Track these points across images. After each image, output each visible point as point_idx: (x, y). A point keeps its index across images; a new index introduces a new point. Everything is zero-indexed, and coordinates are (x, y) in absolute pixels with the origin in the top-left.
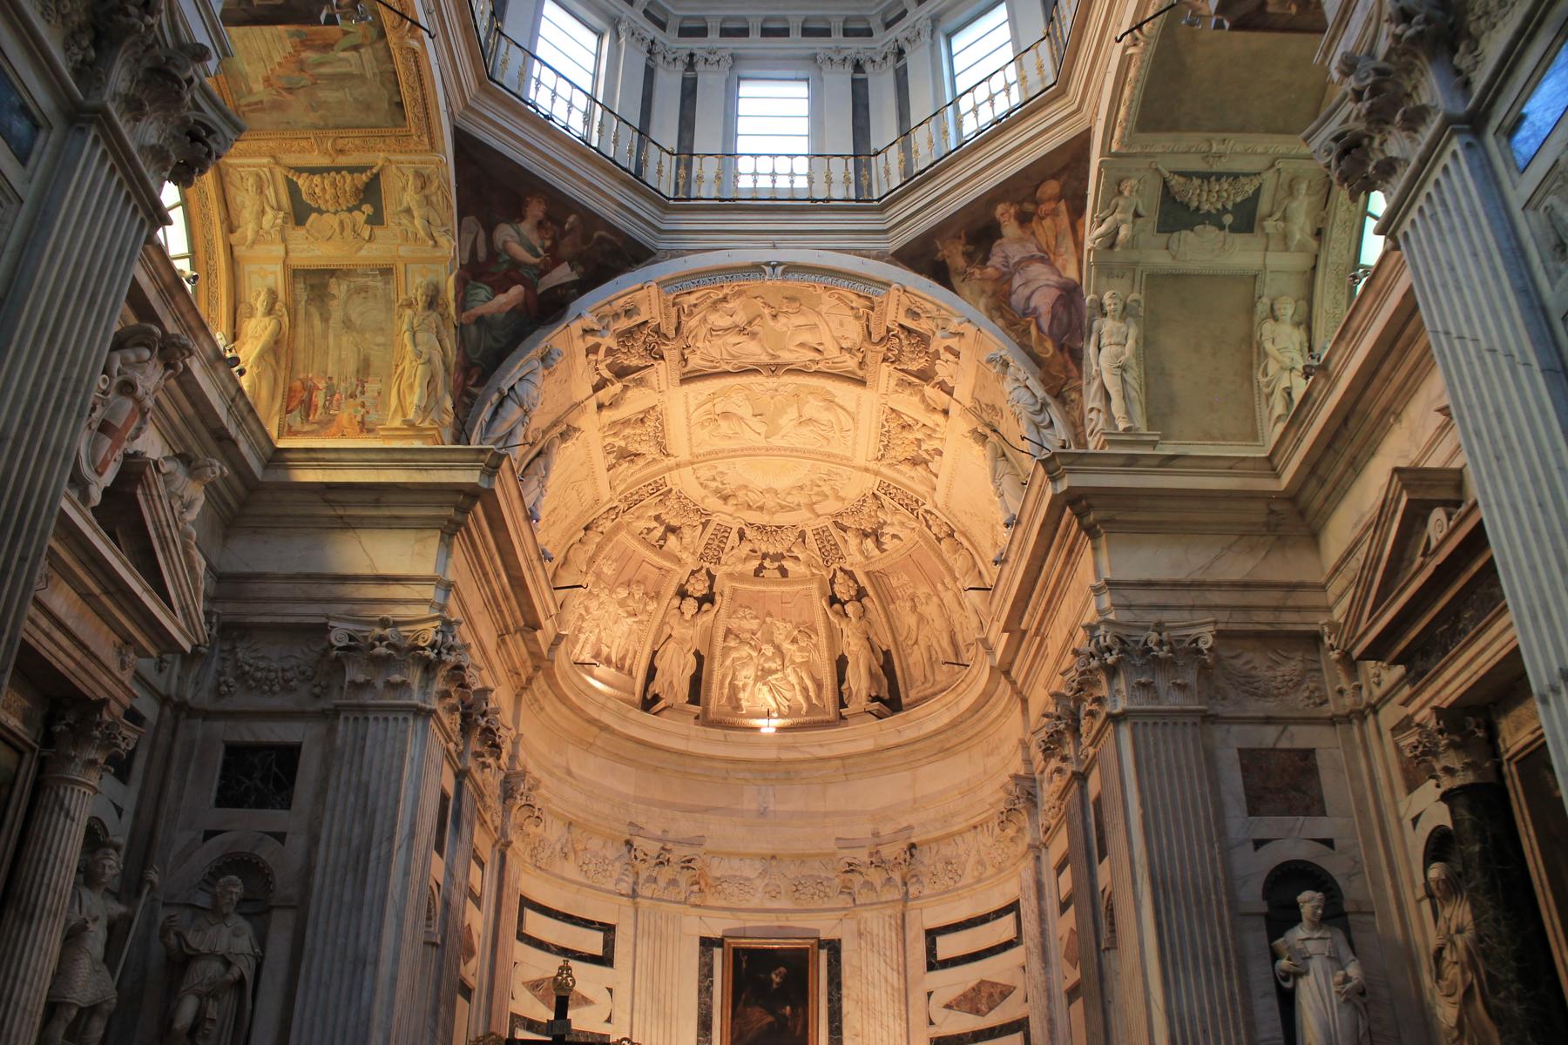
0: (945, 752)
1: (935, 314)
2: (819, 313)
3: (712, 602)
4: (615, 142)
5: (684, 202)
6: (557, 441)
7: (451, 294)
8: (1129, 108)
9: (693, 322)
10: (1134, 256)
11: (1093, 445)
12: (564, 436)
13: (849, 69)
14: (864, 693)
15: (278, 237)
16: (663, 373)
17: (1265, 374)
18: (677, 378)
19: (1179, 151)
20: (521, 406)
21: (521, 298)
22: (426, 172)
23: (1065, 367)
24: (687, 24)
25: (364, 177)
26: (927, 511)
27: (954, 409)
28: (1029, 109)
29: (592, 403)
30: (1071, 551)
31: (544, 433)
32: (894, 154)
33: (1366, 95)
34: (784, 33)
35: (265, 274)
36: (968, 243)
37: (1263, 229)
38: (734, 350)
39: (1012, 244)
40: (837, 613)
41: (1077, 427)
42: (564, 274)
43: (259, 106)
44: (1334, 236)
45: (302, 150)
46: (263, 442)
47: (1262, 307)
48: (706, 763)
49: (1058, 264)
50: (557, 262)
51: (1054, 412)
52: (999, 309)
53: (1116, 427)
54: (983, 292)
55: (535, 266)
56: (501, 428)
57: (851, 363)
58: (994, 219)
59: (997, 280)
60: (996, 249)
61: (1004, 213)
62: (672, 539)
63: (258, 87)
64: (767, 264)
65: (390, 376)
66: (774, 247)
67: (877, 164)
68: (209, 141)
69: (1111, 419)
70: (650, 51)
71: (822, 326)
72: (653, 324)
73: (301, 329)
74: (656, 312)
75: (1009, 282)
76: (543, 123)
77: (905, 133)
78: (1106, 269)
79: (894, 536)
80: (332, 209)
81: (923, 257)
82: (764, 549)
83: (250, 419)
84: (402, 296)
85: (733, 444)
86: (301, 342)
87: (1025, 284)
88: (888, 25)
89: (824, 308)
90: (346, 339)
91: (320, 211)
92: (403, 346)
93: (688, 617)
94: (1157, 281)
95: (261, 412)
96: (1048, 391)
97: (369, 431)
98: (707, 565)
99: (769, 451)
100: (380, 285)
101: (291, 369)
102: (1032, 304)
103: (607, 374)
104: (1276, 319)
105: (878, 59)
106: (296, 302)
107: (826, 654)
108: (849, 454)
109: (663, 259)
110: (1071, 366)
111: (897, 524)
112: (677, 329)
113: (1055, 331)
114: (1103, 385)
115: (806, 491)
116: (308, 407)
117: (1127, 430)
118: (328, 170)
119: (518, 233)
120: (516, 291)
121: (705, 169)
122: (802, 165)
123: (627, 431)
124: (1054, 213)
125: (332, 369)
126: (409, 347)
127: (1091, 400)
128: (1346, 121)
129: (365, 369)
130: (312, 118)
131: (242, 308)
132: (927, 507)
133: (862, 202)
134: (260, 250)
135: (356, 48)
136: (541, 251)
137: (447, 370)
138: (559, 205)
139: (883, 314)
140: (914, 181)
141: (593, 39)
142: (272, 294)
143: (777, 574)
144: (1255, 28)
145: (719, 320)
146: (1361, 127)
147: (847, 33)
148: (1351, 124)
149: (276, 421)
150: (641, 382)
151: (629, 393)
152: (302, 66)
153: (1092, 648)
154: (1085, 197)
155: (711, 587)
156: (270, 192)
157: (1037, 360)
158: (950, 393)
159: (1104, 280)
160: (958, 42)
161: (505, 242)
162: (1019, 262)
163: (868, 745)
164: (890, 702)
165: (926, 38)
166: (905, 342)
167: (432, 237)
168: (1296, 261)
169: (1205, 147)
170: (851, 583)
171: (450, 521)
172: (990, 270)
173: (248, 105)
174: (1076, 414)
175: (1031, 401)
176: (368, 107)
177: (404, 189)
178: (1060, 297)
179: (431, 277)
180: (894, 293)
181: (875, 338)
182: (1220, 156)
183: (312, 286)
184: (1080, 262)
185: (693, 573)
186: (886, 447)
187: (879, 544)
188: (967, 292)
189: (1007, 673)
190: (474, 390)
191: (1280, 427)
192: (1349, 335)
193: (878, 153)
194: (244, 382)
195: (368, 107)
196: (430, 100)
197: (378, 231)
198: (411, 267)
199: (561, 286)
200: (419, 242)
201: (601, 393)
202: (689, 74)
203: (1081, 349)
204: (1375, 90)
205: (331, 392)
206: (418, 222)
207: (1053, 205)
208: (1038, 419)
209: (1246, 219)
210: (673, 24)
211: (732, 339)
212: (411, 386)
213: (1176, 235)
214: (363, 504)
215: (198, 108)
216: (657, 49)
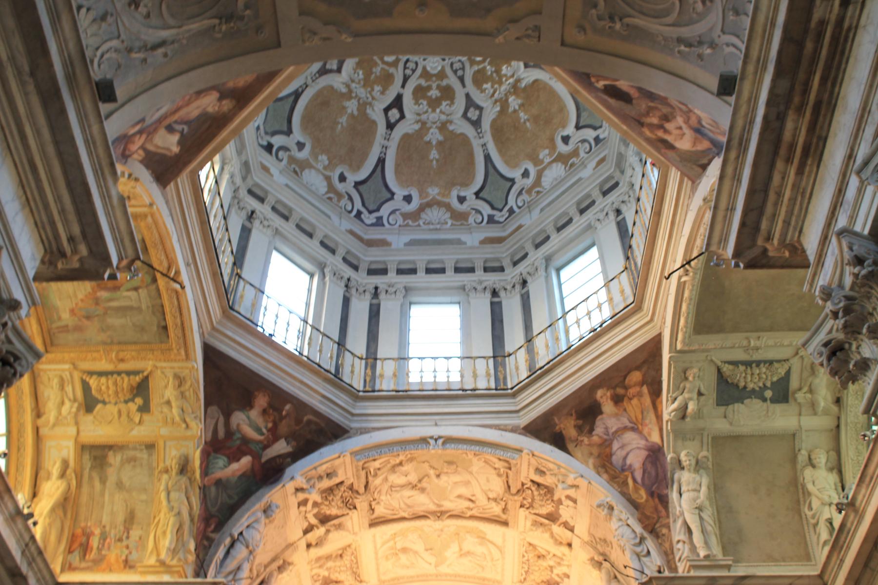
1: (556, 471)
2: (471, 473)
4: (320, 351)
5: (371, 394)
6: (275, 573)
7: (197, 463)
8: (687, 318)
9: (378, 481)
10: (701, 424)
11: (682, 569)
12: (281, 569)
13: (488, 295)
15: (73, 421)
16: (355, 519)
17: (810, 508)
18: (366, 523)
19: (727, 347)
20: (247, 547)
21: (249, 466)
22: (182, 375)
23: (656, 509)
24: (373, 266)
27: (576, 543)
28: (617, 320)
29: (303, 544)
31: (266, 567)
32: (522, 355)
33: (841, 314)
34: (442, 271)
35: (61, 448)
36: (578, 418)
37: (795, 400)
38: (408, 502)
39: (610, 419)
41: (668, 555)
42: (281, 447)
43: (65, 329)
44: (850, 403)
45: (94, 359)
46: (48, 577)
47: (802, 457)
50: (276, 439)
51: (650, 544)
52: (604, 466)
53: (698, 555)
54: (591, 454)
55: (260, 442)
56: (231, 565)
57: (496, 509)
58: (596, 401)
59: (600, 445)
60: (598, 422)
61: (603, 396)
63: (66, 316)
64: (432, 438)
65: (149, 525)
66: (436, 425)
67: (510, 362)
68: (16, 365)
69: (693, 549)
70: (347, 286)
71: (474, 482)
72: (349, 482)
73: (85, 489)
74: (350, 474)
75: (610, 445)
76: (268, 341)
77: (529, 340)
78: (680, 435)
80: (113, 401)
81: (546, 430)
83: (39, 560)
85: (411, 572)
86: (84, 498)
87: (622, 447)
88: (515, 264)
89: (474, 469)
90: (119, 497)
91: (104, 403)
92: (160, 502)
94: (719, 442)
95: (48, 556)
96: (645, 528)
97: (132, 567)
99: (438, 577)
101: (75, 519)
102: (628, 462)
103: (314, 521)
104: (814, 466)
105: (509, 287)
106: (82, 469)
108: (499, 578)
109: (355, 434)
110: (660, 508)
112: (366, 487)
113: (647, 481)
114: (685, 523)
116: (85, 548)
117: (707, 557)
118: (112, 373)
119: (248, 418)
120: (246, 460)
121: (386, 369)
122: (456, 365)
123: (330, 564)
124: (640, 395)
125: (106, 519)
126: (164, 503)
127: (677, 534)
128: (830, 332)
129: (130, 519)
130: (102, 337)
131: (42, 474)
133: (501, 390)
134: (59, 430)
135: (136, 289)
136: (264, 430)
137: (192, 520)
138: (279, 398)
139: (518, 472)
140: (537, 374)
141: (308, 277)
142: (65, 464)
144: (762, 267)
145: (396, 479)
146: (841, 336)
147: (486, 270)
148: (834, 334)
149: (60, 560)
150: (339, 527)
151: (331, 536)
152: (97, 302)
154: (660, 383)
156: (69, 389)
157: (635, 505)
158: (572, 530)
159: (680, 443)
160: (565, 273)
161: (238, 425)
162: (616, 432)
165: (542, 272)
166: (536, 493)
167: (185, 421)
168: (824, 422)
169: (745, 343)
172: (595, 439)
173: (58, 328)
174: (667, 545)
175: (633, 536)
176: (143, 329)
177: (166, 387)
178: (648, 457)
179: (184, 451)
180: (525, 456)
181: (514, 490)
182: (757, 349)
183: (95, 458)
184: (661, 430)
186: (526, 572)
188: (579, 455)
190: (212, 535)
191: (827, 549)
192: (868, 479)
193: (510, 355)
194: (38, 532)
195: (143, 329)
196: (186, 325)
197: (146, 417)
198: (168, 443)
199: (280, 456)
200: (177, 425)
202: (375, 301)
203: (667, 496)
204: (847, 311)
205: (104, 537)
206: (175, 411)
207: (638, 389)
208: (638, 549)
209: (782, 393)
210: (363, 267)
211: (407, 493)
212: (164, 533)
213: (731, 407)
215: (9, 341)
216: (351, 284)
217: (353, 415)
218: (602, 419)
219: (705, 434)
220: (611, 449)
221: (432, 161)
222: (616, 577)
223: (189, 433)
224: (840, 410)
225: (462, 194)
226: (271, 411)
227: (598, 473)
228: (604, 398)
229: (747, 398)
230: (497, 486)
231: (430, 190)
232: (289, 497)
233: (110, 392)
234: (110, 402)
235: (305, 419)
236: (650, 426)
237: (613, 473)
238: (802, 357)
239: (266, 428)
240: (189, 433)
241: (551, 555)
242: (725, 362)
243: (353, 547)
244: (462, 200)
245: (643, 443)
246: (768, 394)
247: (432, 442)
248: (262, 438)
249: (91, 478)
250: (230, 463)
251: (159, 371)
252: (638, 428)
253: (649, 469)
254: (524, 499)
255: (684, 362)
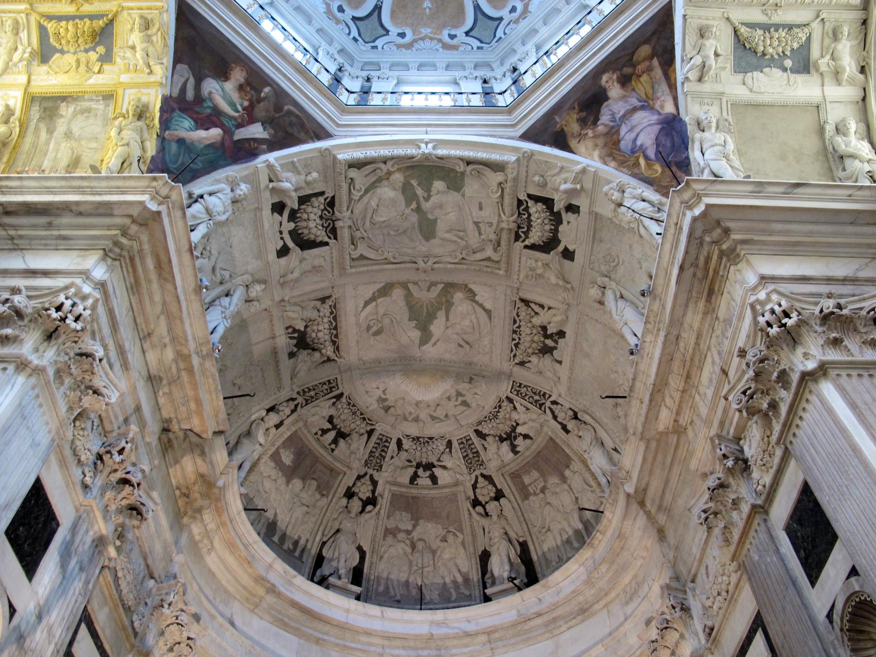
0: (584, 612)
2: (463, 195)
3: (375, 505)
10: (719, 88)
14: (506, 575)
21: (219, 138)
22: (149, 17)
25: (101, 22)
26: (554, 403)
30: (711, 292)
36: (581, 111)
37: (817, 70)
40: (479, 514)
42: (256, 131)
47: (829, 129)
48: (363, 639)
49: (657, 106)
50: (252, 121)
52: (610, 155)
54: (596, 145)
57: (489, 252)
58: (601, 87)
59: (607, 134)
62: (342, 442)
64: (421, 141)
72: (329, 194)
73: (29, 139)
75: (618, 132)
79: (526, 437)
80: (72, 50)
82: (418, 460)
84: (118, 111)
91: (62, 52)
93: (353, 515)
94: (741, 107)
98: (370, 471)
100: (101, 107)
102: (639, 143)
103: (290, 244)
106: (29, 120)
107: (472, 549)
110: (679, 174)
111: (529, 419)
115: (453, 403)
119: (223, 90)
120: (215, 133)
124: (650, 69)
125: (46, 164)
132: (551, 399)
138: (255, 80)
143: (428, 482)
153: (768, 316)
155: (373, 492)
157: (649, 182)
161: (210, 93)
162: (624, 116)
163: (510, 616)
164: (529, 573)
166: (532, 210)
170: (490, 487)
171: (116, 244)
172: (600, 128)
179: (144, 99)
183: (45, 109)
185: (359, 477)
186: (516, 345)
187: (514, 449)
189: (642, 504)
197: (107, 67)
201: (283, 261)
203: (688, 158)
206: (139, 55)
207: (647, 63)
213: (749, 74)
214: (35, 227)
217: (338, 125)
218: (607, 106)
219: (724, 100)
220: (619, 134)
221: (425, 9)
222: (622, 297)
223: (152, 79)
224: (866, 77)
225: (453, 33)
226: (248, 89)
227: (605, 163)
228: (611, 82)
229: (766, 67)
230: (489, 214)
231: (423, 30)
232: (262, 186)
233: (69, 36)
234: (69, 52)
235: (286, 108)
236: (662, 98)
237: (622, 158)
238: (823, 19)
239: (241, 105)
240: (152, 79)
241: (546, 309)
242: (743, 24)
243: (333, 298)
244: (452, 37)
245: (655, 117)
246: (788, 63)
247: (423, 146)
248: (236, 114)
249: (37, 129)
250: (197, 129)
251: (125, 12)
252: (649, 105)
253: (663, 142)
254: (519, 227)
255: (699, 18)
